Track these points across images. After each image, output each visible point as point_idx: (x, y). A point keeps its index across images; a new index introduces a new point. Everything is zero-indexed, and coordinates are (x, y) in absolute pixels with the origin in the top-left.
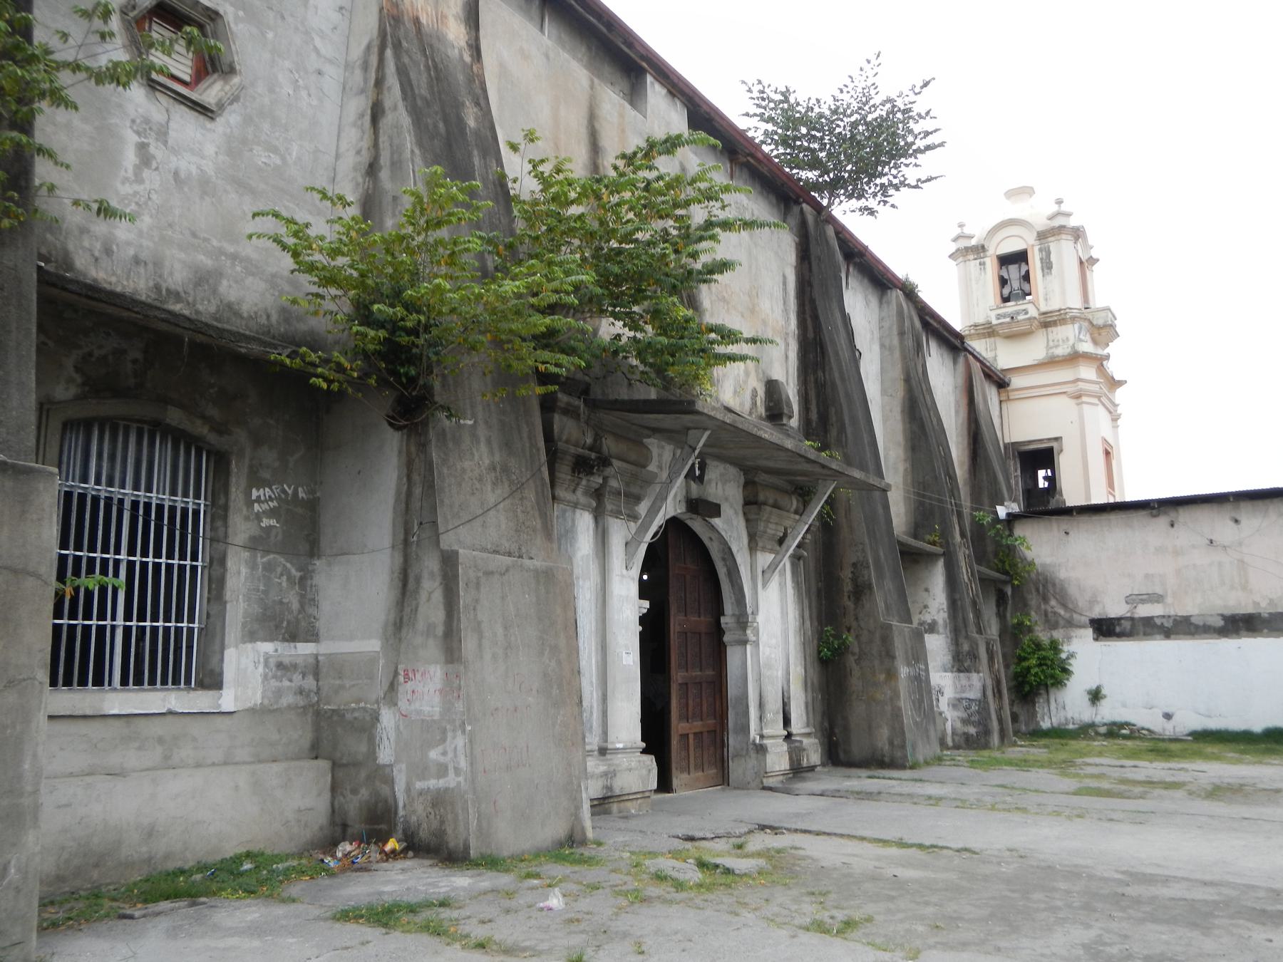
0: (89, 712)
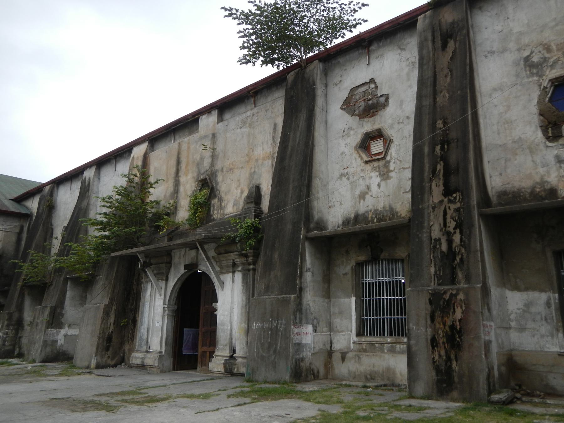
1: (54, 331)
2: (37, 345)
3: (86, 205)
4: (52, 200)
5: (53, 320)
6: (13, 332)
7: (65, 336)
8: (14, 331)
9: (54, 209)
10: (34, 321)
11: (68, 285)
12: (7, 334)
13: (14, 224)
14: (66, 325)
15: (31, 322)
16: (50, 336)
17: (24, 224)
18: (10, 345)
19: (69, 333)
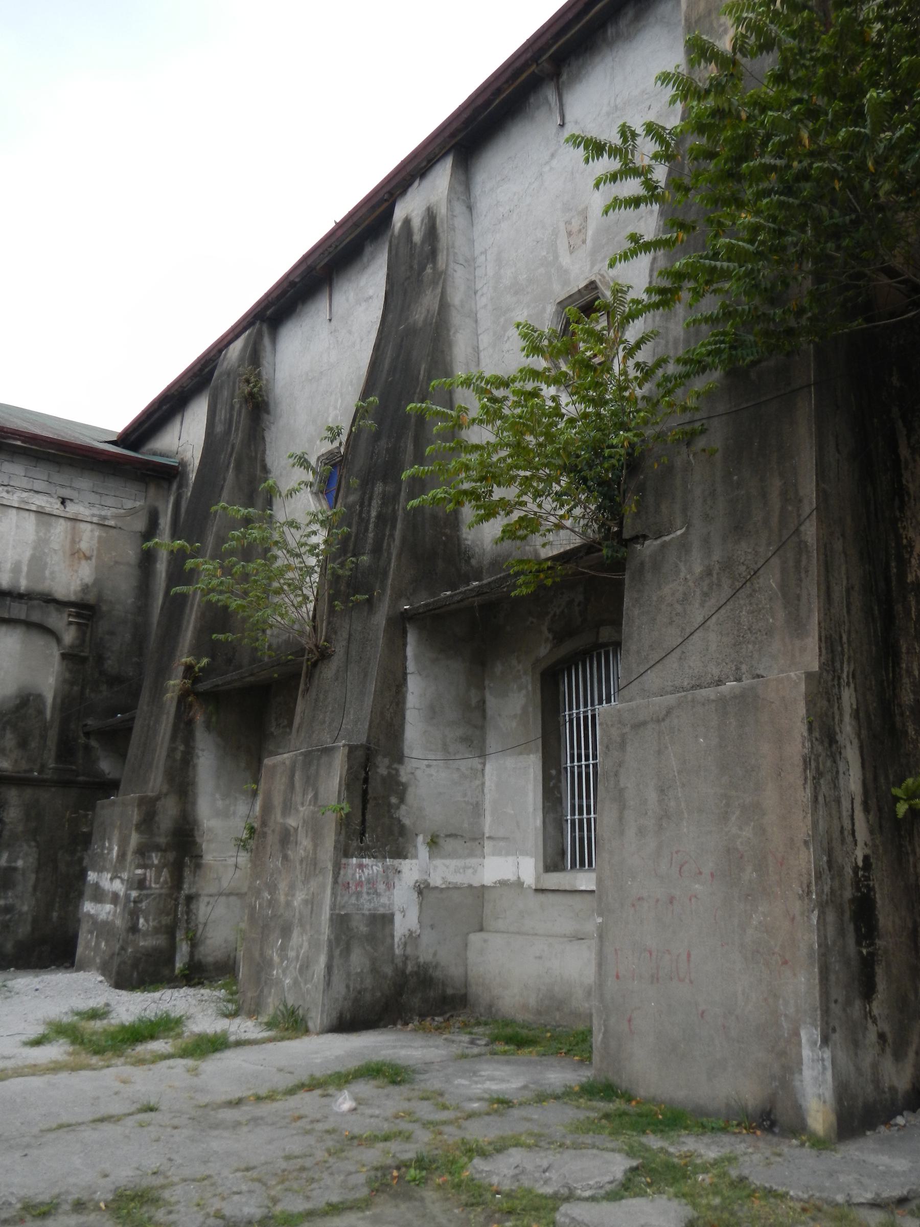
0: (568, 888)
1: (373, 867)
2: (299, 940)
3: (436, 306)
4: (259, 376)
5: (364, 815)
6: (162, 879)
7: (422, 889)
8: (165, 873)
9: (268, 412)
10: (264, 824)
11: (410, 651)
12: (141, 884)
13: (129, 504)
14: (420, 838)
15: (252, 830)
16: (358, 894)
17: (160, 506)
18: (157, 931)
19: (436, 880)
